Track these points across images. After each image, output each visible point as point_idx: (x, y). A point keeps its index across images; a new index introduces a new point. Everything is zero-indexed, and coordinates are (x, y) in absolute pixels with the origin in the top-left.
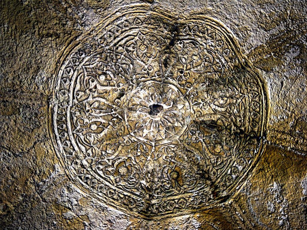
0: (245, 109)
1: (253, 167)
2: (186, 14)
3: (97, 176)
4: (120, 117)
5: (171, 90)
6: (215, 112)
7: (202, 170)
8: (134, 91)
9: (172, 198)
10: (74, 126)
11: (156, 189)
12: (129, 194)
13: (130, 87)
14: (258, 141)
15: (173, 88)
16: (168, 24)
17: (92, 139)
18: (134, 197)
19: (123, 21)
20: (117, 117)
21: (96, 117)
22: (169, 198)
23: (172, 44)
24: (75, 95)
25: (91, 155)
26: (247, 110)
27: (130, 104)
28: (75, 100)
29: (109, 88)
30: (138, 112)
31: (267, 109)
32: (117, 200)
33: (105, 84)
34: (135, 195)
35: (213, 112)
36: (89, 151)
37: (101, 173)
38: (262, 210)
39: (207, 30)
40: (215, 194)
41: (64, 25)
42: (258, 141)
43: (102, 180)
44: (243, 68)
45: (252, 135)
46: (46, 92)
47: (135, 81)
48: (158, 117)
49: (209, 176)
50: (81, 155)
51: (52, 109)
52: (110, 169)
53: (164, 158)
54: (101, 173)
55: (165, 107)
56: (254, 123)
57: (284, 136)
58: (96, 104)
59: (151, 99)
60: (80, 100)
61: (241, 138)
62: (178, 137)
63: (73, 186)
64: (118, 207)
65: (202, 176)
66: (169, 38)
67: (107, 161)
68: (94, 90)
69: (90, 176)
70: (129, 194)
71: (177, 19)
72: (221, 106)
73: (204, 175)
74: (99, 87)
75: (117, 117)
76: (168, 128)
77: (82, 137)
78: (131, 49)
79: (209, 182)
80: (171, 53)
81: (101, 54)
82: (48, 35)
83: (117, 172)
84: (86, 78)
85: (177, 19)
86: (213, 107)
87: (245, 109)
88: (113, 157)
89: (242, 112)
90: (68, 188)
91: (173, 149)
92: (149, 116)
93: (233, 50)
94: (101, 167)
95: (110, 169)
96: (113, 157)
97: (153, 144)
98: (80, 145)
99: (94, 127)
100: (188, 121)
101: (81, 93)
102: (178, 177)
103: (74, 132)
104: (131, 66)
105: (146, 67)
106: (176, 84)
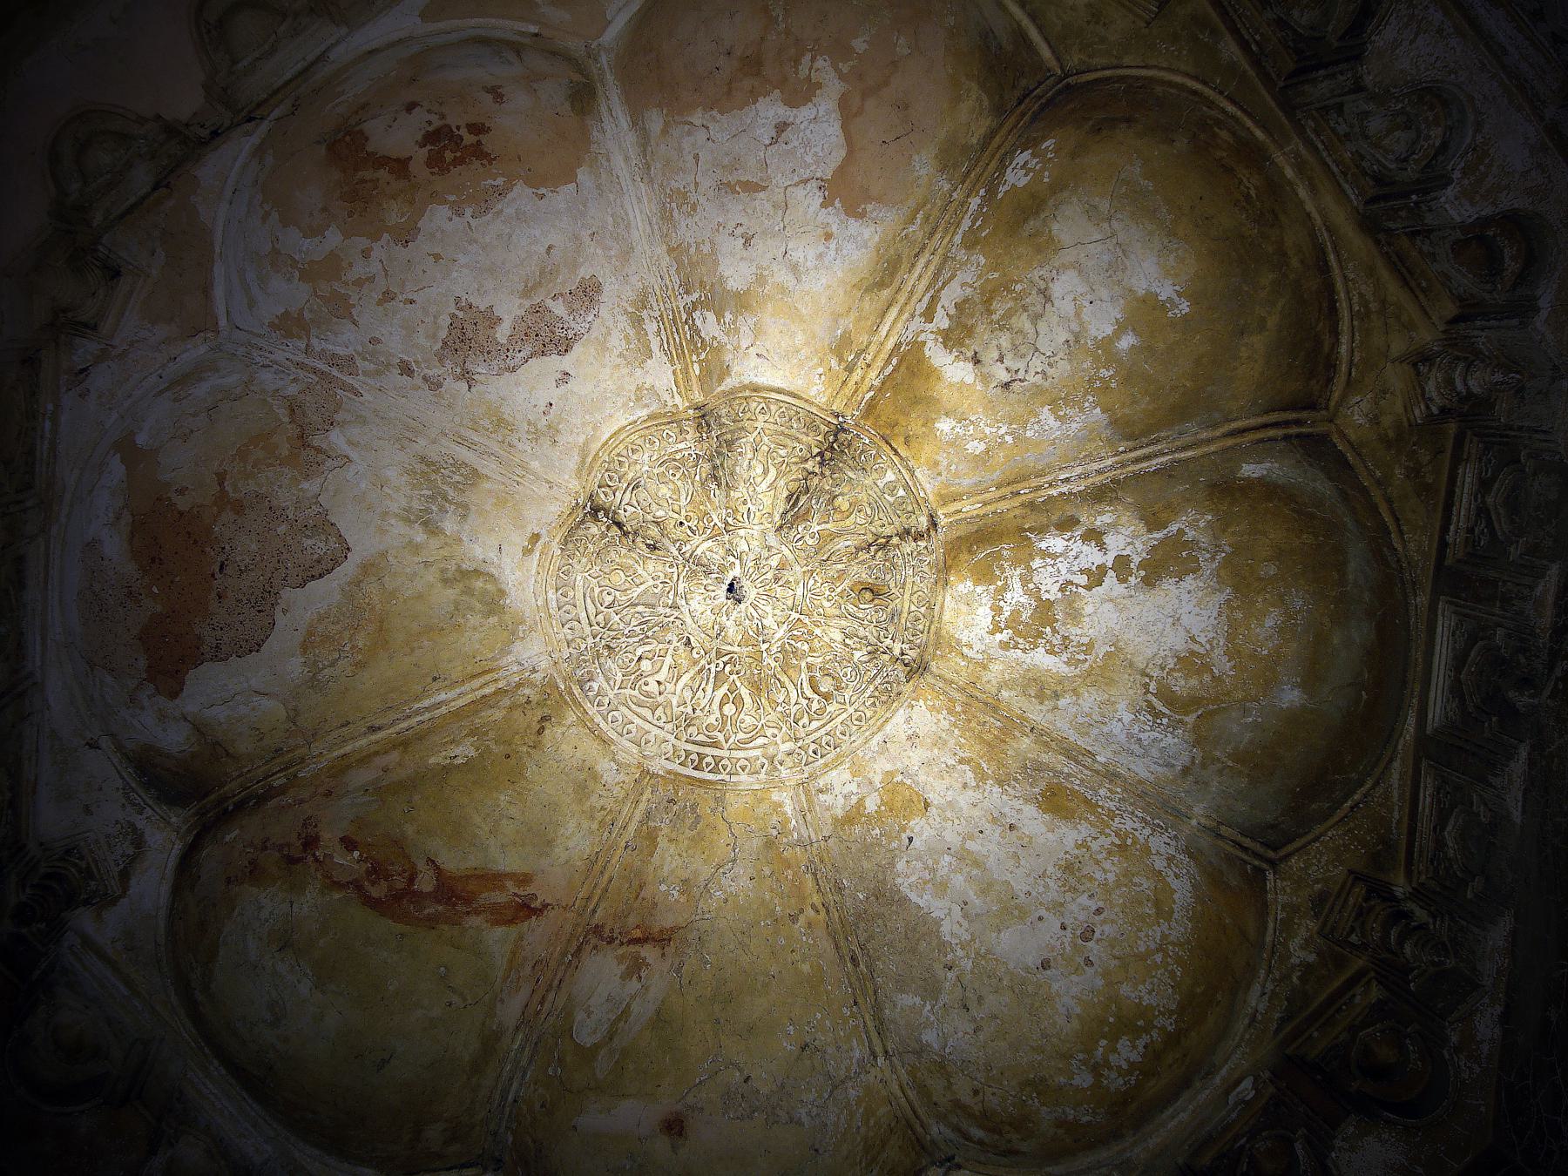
0: (782, 433)
1: (896, 453)
2: (574, 485)
3: (817, 735)
4: (725, 659)
5: (708, 553)
6: (772, 486)
7: (870, 545)
8: (689, 620)
9: (905, 615)
10: (715, 745)
11: (878, 639)
12: (872, 688)
13: (678, 622)
14: (844, 430)
15: (703, 547)
16: (582, 522)
17: (749, 720)
18: (878, 680)
19: (554, 597)
20: (725, 664)
21: (711, 701)
22: (903, 621)
23: (619, 525)
24: (658, 724)
25: (776, 731)
26: (786, 431)
27: (710, 632)
28: (669, 726)
29: (668, 660)
30: (728, 623)
31: (794, 396)
32: (875, 712)
33: (659, 664)
34: (876, 676)
35: (773, 492)
36: (769, 732)
37: (815, 724)
38: (981, 461)
39: (619, 455)
40: (919, 536)
41: (529, 702)
42: (844, 430)
43: (828, 728)
44: (703, 416)
45: (831, 439)
46: (633, 770)
47: (668, 610)
48: (750, 591)
49: (883, 537)
50: (771, 750)
51: (669, 772)
52: (815, 706)
53: (829, 604)
54: (815, 724)
55: (737, 572)
56: (811, 426)
57: (851, 383)
58: (688, 694)
59: (713, 594)
60: (669, 720)
61: (831, 459)
62: (798, 568)
63: (821, 783)
64: (888, 715)
65: (883, 547)
66: (608, 528)
67: (797, 707)
68: (662, 687)
69: (813, 747)
70: (872, 688)
71: (577, 504)
72: (766, 472)
73: (882, 544)
74: (661, 676)
75: (725, 664)
76: (777, 580)
77: (741, 736)
78: (609, 599)
79: (895, 540)
80: (636, 533)
81: (599, 656)
82: (541, 731)
83: (827, 697)
84: (636, 693)
85: (577, 504)
86: (764, 486)
87: (782, 433)
88: (793, 695)
89: (789, 442)
90: (821, 791)
91: (819, 585)
92: (743, 606)
93: (669, 423)
94: (805, 720)
95: (815, 706)
96: (793, 695)
97: (795, 615)
98: (751, 745)
99: (729, 709)
100: (772, 540)
101: (659, 712)
102: (872, 591)
103: (726, 746)
104: (640, 608)
105: (651, 582)
106: (700, 541)
